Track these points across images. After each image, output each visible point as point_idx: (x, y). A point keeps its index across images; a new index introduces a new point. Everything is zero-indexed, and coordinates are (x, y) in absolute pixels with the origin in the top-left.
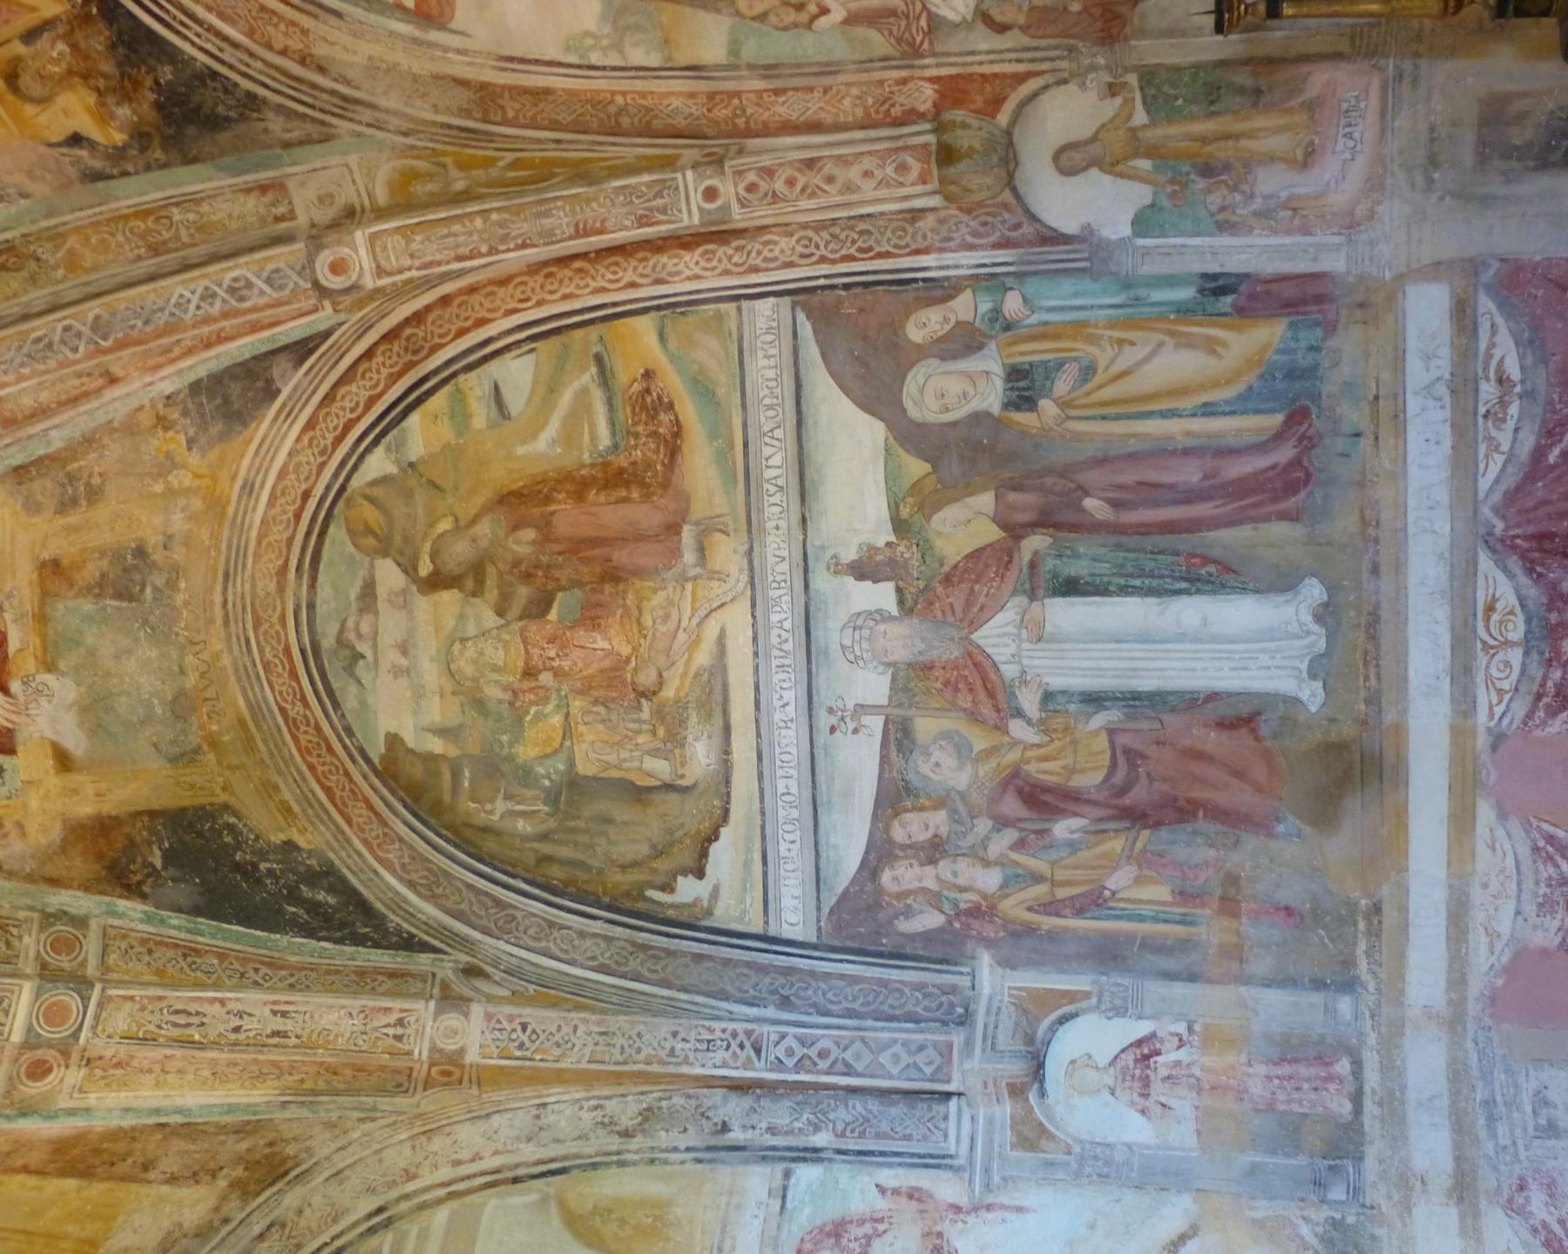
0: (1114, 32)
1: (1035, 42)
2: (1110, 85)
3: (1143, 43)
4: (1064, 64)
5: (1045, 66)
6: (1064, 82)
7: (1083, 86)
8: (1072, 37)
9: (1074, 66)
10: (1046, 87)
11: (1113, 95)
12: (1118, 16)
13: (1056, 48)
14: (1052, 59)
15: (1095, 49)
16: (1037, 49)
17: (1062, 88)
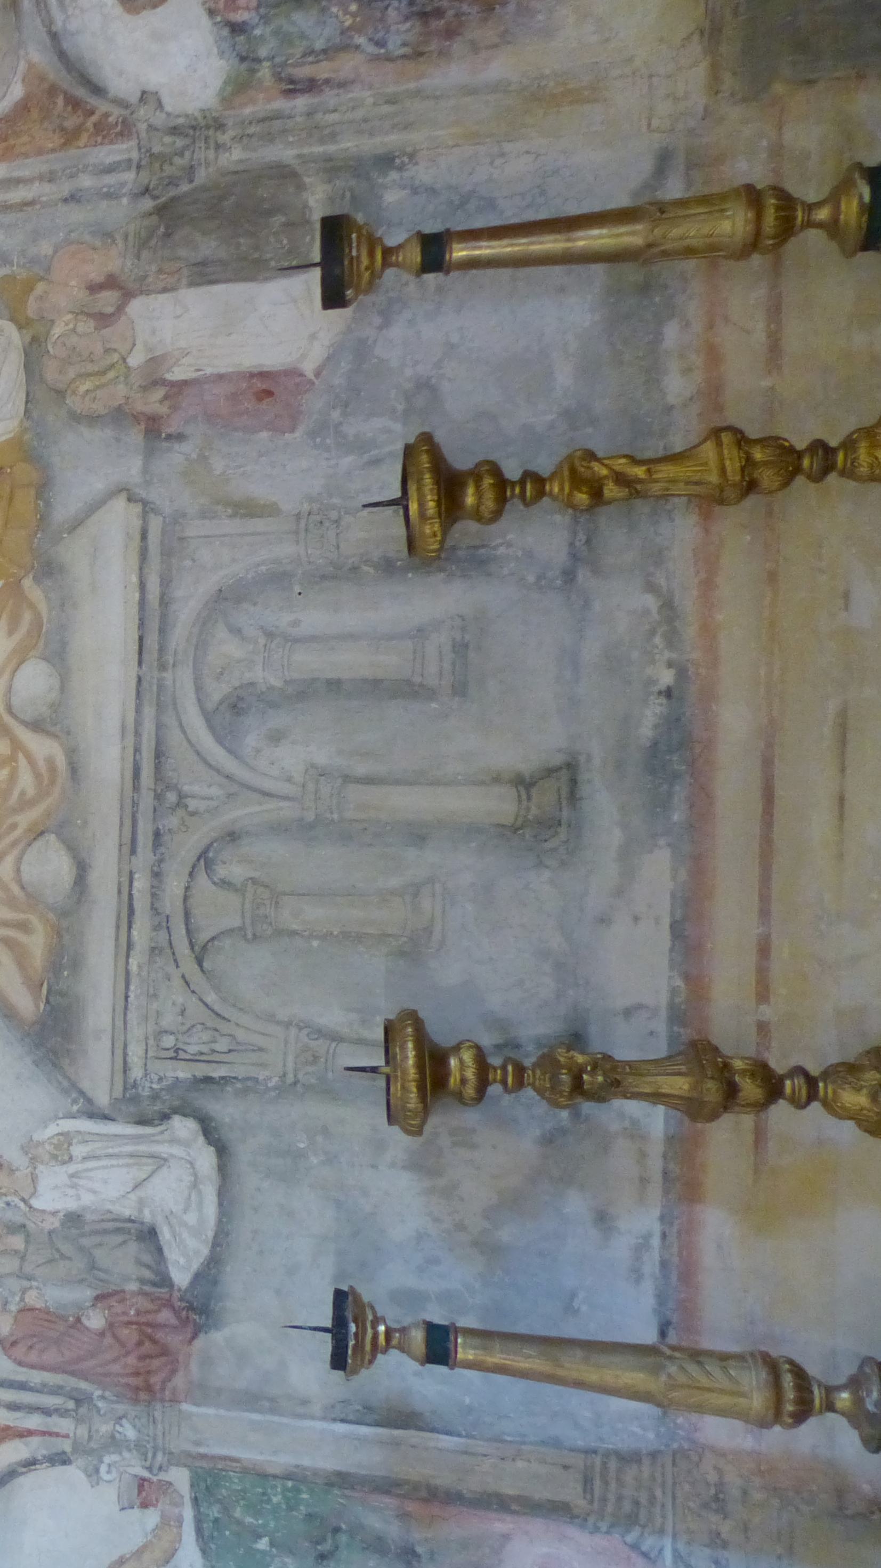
0: (155, 1380)
1: (22, 1374)
2: (142, 1483)
3: (203, 1410)
4: (64, 1425)
5: (33, 1422)
6: (61, 1459)
7: (93, 1474)
8: (83, 1376)
9: (82, 1431)
10: (31, 1463)
11: (145, 1505)
12: (164, 1352)
13: (56, 1391)
14: (46, 1412)
15: (121, 1408)
16: (22, 1386)
17: (59, 1469)
